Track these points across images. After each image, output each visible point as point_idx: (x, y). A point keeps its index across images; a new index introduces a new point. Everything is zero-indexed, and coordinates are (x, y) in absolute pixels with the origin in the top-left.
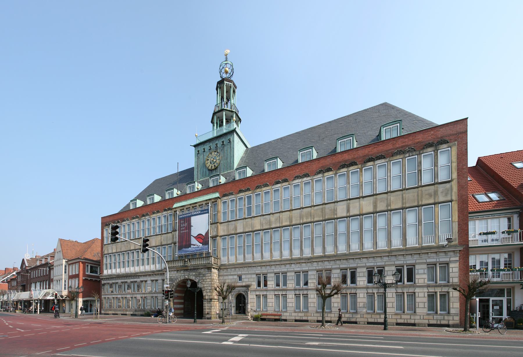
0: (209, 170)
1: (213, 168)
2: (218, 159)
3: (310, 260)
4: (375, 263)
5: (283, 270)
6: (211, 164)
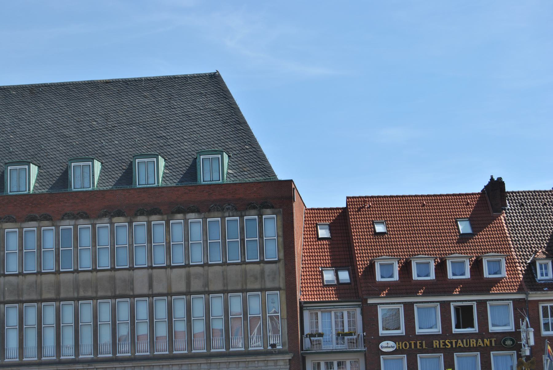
3: (92, 366)
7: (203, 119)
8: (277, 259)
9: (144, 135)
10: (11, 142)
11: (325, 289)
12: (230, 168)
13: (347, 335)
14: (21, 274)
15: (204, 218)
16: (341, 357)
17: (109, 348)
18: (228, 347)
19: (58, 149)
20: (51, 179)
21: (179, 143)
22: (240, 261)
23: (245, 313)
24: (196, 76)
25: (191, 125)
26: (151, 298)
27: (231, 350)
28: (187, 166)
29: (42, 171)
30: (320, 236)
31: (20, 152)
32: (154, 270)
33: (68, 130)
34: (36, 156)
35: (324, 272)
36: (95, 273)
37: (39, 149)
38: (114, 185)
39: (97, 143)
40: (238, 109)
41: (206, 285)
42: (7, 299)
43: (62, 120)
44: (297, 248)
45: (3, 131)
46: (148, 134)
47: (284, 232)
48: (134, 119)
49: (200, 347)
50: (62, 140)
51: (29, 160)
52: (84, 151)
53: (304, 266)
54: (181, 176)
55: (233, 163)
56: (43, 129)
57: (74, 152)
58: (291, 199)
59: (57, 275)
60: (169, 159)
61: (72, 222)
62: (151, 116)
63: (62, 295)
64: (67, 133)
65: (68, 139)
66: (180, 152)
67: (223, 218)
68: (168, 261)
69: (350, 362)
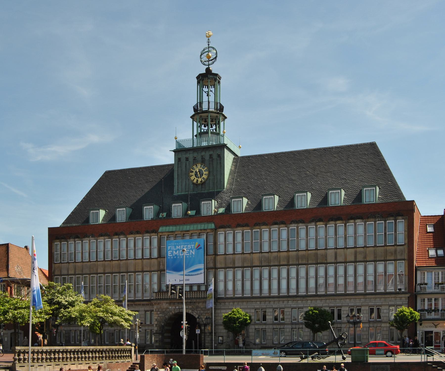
0: (193, 184)
1: (199, 183)
2: (205, 174)
4: (355, 304)
5: (280, 306)
6: (196, 177)
7: (366, 168)
8: (404, 244)
9: (334, 178)
10: (265, 184)
11: (430, 259)
12: (380, 194)
13: (440, 284)
14: (270, 252)
15: (365, 222)
16: (436, 296)
18: (375, 289)
19: (289, 187)
20: (285, 203)
21: (353, 182)
22: (383, 245)
23: (385, 272)
24: (362, 144)
25: (359, 172)
26: (336, 264)
27: (377, 291)
28: (357, 194)
29: (281, 199)
30: (428, 231)
31: (269, 189)
32: (338, 250)
33: (294, 177)
34: (278, 191)
35: (429, 250)
36: (307, 251)
37: (279, 187)
39: (309, 183)
40: (385, 162)
41: (365, 257)
42: (263, 264)
43: (291, 171)
44: (415, 237)
45: (261, 178)
46: (336, 177)
47: (408, 229)
48: (329, 169)
49: (361, 289)
50: (291, 182)
51: (274, 193)
52: (302, 187)
53: (419, 247)
54: (353, 200)
55: (382, 192)
56: (281, 176)
57: (297, 188)
58: (413, 211)
59: (288, 252)
60: (347, 190)
61: (296, 225)
62: (338, 168)
63: (290, 263)
64: (294, 178)
65: (294, 181)
66: (353, 186)
67: (375, 222)
68: (345, 244)
69: (442, 299)
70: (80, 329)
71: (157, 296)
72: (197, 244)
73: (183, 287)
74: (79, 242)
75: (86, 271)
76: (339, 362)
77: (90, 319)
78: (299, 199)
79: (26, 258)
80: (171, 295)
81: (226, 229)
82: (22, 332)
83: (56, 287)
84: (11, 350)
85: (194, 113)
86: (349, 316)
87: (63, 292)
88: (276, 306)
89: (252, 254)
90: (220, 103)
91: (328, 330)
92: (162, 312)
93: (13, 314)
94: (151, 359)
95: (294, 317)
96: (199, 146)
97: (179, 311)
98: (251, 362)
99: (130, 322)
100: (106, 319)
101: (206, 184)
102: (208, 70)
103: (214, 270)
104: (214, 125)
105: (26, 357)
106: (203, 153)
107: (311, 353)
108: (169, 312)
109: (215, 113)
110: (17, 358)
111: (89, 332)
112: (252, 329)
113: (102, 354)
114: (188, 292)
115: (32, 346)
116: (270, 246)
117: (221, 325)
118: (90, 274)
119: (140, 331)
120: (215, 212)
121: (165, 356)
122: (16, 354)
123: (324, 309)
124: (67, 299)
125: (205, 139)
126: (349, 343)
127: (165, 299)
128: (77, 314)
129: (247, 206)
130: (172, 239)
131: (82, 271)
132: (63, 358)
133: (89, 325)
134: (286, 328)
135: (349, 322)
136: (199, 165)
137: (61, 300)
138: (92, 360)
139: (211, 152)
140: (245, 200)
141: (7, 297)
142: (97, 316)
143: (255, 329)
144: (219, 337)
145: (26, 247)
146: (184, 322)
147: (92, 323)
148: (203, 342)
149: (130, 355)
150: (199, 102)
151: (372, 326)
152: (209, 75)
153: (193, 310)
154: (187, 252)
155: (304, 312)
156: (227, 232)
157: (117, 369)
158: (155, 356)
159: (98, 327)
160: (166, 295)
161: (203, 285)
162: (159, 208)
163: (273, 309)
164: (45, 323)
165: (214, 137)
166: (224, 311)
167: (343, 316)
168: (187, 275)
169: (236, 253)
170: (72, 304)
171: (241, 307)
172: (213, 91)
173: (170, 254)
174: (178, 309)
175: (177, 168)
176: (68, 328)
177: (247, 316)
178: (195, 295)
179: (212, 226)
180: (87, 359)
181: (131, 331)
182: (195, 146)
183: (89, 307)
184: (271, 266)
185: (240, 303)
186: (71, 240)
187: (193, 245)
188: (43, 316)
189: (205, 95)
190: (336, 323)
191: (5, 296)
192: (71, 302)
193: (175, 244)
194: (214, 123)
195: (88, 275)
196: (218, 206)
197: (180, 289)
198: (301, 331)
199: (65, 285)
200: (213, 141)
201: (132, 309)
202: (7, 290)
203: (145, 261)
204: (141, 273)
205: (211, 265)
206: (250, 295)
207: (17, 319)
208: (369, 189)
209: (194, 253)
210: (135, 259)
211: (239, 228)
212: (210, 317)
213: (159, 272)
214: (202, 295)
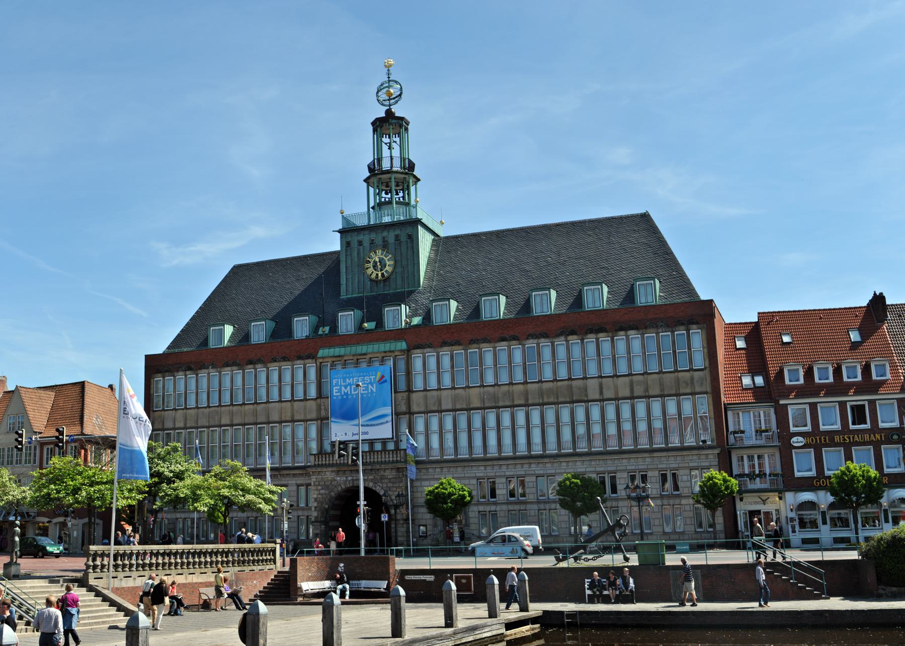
0: (371, 280)
1: (379, 278)
2: (389, 265)
6: (375, 270)
17: (570, 445)
18: (667, 443)
26: (602, 403)
27: (670, 445)
32: (604, 379)
36: (555, 383)
38: (568, 309)
41: (647, 390)
42: (486, 405)
61: (535, 341)
63: (530, 402)
70: (191, 516)
71: (317, 460)
72: (379, 375)
73: (358, 444)
74: (192, 376)
75: (203, 422)
76: (619, 565)
77: (209, 500)
78: (538, 300)
79: (110, 404)
80: (339, 457)
81: (425, 350)
82: (101, 522)
83: (155, 449)
84: (82, 552)
85: (369, 174)
86: (630, 488)
87: (166, 456)
88: (512, 473)
89: (467, 389)
90: (409, 159)
91: (598, 512)
92: (325, 487)
93: (88, 494)
94: (308, 565)
95: (541, 491)
96: (378, 222)
97: (353, 484)
98: (474, 567)
99: (274, 505)
100: (234, 500)
101: (391, 280)
102: (389, 113)
103: (407, 416)
104: (401, 191)
105: (106, 562)
106: (385, 234)
107: (573, 550)
108: (336, 486)
109: (402, 173)
110: (92, 564)
111: (206, 522)
112: (473, 512)
113: (227, 557)
114: (366, 452)
115: (115, 545)
116: (496, 376)
117: (422, 506)
118: (208, 427)
119: (289, 518)
120: (406, 323)
121: (330, 558)
122: (91, 558)
123: (589, 477)
124: (173, 468)
125: (388, 212)
126: (632, 532)
127: (329, 465)
128: (188, 492)
129: (457, 313)
130: (339, 367)
131: (197, 422)
132: (164, 564)
133: (206, 509)
134: (530, 510)
135: (629, 497)
136: (379, 252)
137: (163, 469)
138: (211, 567)
139: (398, 232)
140: (454, 304)
141: (80, 465)
142: (219, 495)
143: (479, 512)
144: (420, 526)
145: (111, 387)
146: (362, 502)
147: (212, 506)
148: (393, 534)
149: (273, 558)
150: (376, 157)
151: (667, 504)
152: (390, 120)
153: (375, 481)
154: (364, 388)
155: (557, 482)
156: (427, 354)
157: (252, 582)
158: (314, 559)
159: (221, 513)
160: (331, 459)
161: (391, 440)
162: (317, 319)
163: (507, 478)
164: (136, 507)
165: (401, 209)
166: (427, 483)
167: (620, 487)
168: (365, 426)
169: (442, 388)
170: (180, 476)
171: (455, 476)
172: (398, 142)
173: (336, 393)
174: (351, 481)
175: (345, 257)
176: (173, 516)
177: (465, 490)
178: (378, 458)
179: (403, 345)
180: (203, 566)
181: (275, 518)
182: (372, 223)
183: (207, 481)
184: (500, 407)
185: (452, 469)
186: (181, 373)
187: (372, 377)
188: (134, 495)
189: (385, 148)
190: (609, 499)
191: (77, 464)
192: (178, 473)
193: (345, 375)
194: (401, 187)
195: (205, 429)
196: (411, 314)
197: (353, 448)
198: (553, 515)
199: (170, 446)
200: (400, 215)
201: (276, 483)
202: (80, 454)
203: (296, 403)
204: (290, 424)
205: (403, 408)
206: (468, 456)
207: (93, 501)
208: (645, 282)
209: (374, 390)
210: (280, 401)
211: (446, 348)
212: (404, 493)
213: (319, 421)
214: (389, 457)
